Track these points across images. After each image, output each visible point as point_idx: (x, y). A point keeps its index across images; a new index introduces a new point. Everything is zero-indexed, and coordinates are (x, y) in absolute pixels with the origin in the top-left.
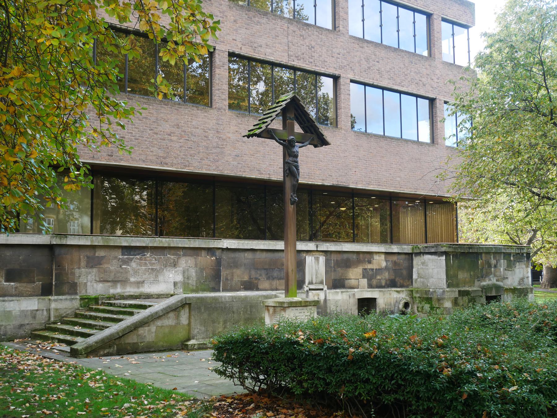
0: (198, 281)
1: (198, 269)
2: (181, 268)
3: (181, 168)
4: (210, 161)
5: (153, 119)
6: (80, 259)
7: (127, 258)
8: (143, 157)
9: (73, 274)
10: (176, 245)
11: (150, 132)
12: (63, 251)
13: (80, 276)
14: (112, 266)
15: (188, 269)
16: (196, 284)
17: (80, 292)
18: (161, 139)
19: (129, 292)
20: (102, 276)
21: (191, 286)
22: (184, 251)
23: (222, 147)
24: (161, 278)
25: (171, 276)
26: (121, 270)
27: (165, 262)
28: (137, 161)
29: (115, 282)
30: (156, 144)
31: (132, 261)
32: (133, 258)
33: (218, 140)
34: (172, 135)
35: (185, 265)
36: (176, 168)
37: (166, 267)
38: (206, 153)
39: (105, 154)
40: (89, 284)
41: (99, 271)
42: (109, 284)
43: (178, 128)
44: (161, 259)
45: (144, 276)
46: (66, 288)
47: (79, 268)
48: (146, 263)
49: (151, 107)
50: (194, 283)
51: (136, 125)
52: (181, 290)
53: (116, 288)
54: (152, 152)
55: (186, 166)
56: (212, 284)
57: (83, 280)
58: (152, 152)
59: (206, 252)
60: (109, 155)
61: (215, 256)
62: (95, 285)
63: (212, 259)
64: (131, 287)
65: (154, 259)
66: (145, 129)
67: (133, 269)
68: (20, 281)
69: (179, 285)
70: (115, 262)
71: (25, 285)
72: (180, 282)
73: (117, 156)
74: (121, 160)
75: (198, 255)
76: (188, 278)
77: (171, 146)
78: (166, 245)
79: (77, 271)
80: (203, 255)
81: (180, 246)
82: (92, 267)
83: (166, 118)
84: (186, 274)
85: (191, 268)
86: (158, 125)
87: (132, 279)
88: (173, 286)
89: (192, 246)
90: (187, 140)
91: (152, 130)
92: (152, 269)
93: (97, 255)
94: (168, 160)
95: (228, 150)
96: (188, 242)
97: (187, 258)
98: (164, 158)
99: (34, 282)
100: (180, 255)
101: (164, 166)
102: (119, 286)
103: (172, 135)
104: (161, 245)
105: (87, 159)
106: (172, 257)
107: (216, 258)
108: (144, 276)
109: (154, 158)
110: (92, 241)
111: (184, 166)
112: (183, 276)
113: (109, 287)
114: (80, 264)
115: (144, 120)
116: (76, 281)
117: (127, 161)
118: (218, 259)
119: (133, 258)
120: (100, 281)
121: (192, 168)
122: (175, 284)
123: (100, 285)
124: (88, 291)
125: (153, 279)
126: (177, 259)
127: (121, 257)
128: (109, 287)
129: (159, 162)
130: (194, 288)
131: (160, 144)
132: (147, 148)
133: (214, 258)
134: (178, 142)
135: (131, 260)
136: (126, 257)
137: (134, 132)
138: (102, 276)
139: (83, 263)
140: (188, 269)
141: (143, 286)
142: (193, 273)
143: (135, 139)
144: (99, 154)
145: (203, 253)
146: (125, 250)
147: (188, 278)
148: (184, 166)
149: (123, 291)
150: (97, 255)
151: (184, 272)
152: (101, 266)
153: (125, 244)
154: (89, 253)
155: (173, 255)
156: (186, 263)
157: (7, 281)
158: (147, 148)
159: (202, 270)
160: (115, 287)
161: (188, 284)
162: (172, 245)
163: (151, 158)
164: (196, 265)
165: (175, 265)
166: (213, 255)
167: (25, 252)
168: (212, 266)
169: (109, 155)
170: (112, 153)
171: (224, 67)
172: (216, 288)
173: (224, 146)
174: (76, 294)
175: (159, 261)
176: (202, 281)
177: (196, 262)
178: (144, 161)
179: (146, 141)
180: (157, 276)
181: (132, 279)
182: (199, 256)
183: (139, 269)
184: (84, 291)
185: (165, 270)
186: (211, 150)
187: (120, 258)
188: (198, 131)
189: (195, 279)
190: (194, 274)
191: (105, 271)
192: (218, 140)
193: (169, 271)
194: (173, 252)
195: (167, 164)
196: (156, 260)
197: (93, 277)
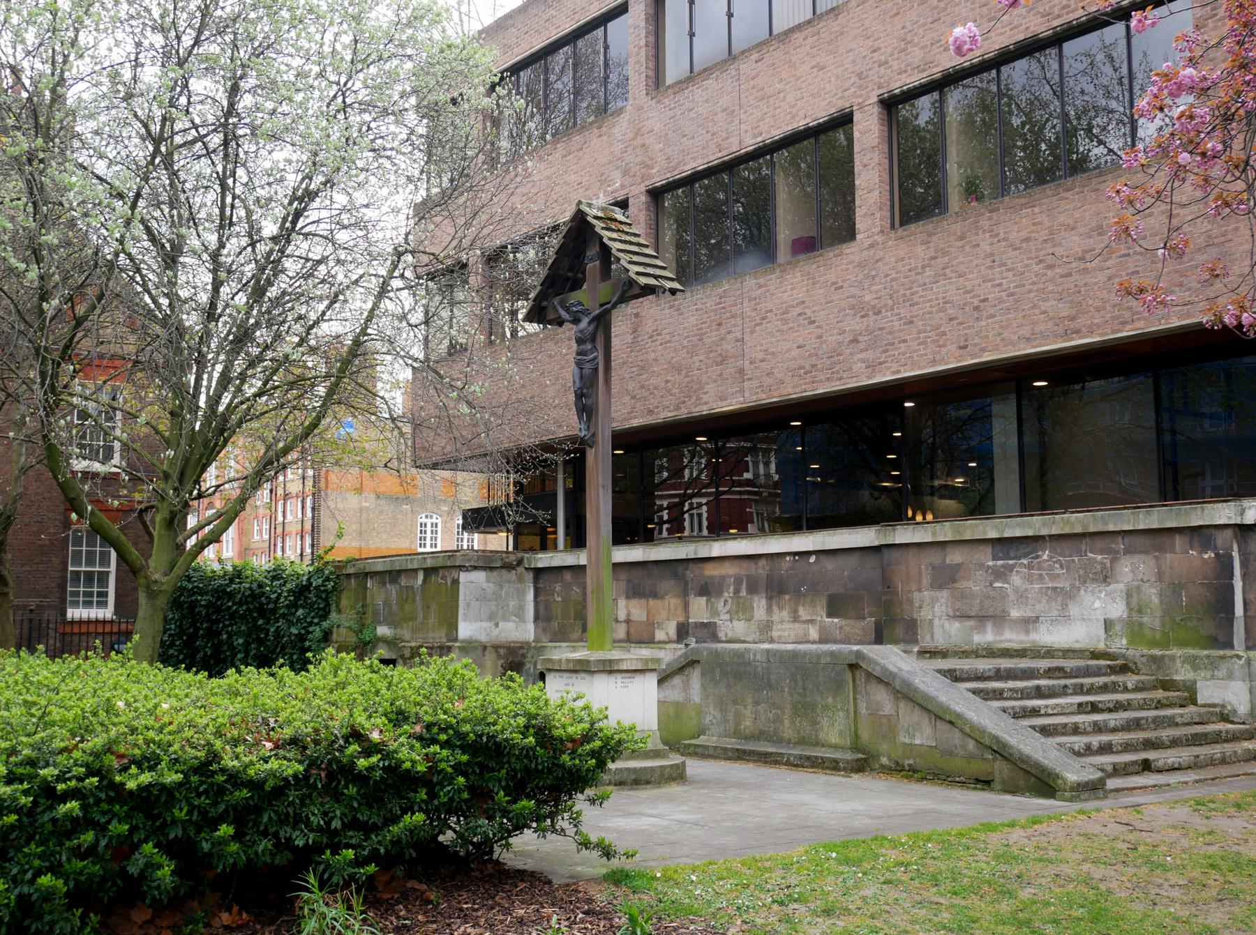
0: (1167, 619)
1: (1164, 586)
2: (1121, 586)
3: (1113, 332)
4: (1189, 289)
5: (1043, 235)
6: (920, 573)
7: (1003, 566)
8: (1025, 332)
9: (910, 601)
10: (1100, 528)
11: (1036, 268)
12: (895, 554)
13: (921, 607)
14: (975, 585)
15: (1138, 588)
16: (1163, 625)
17: (923, 638)
18: (1062, 276)
19: (1010, 641)
20: (959, 605)
21: (1147, 632)
22: (1127, 540)
23: (1222, 239)
24: (1074, 610)
25: (1097, 604)
26: (992, 593)
27: (1082, 572)
28: (1013, 344)
29: (982, 619)
30: (1052, 292)
31: (1011, 571)
32: (1013, 566)
33: (1209, 227)
34: (1088, 257)
35: (1131, 575)
36: (1101, 335)
37: (1085, 582)
38: (1176, 272)
39: (953, 348)
40: (936, 622)
41: (953, 596)
42: (972, 623)
43: (1100, 234)
44: (1072, 565)
45: (1037, 607)
46: (899, 631)
47: (920, 590)
48: (1041, 575)
49: (1037, 210)
50: (1157, 624)
51: (1009, 262)
52: (1124, 642)
53: (984, 632)
54: (1044, 312)
55: (1125, 323)
56: (1208, 627)
57: (925, 614)
58: (1044, 312)
59: (1187, 539)
60: (961, 348)
61: (1215, 549)
62: (947, 624)
63: (1206, 556)
64: (1012, 629)
65: (1057, 566)
66: (1026, 266)
67: (1016, 591)
68: (846, 618)
69: (1118, 627)
70: (980, 574)
71: (851, 622)
72: (1120, 620)
73: (975, 345)
74: (983, 350)
75: (1162, 549)
76: (1140, 611)
77: (1085, 285)
78: (1078, 529)
79: (916, 595)
80: (1178, 549)
81: (1111, 528)
82: (940, 587)
83: (1071, 221)
84: (1135, 600)
85: (1147, 585)
86: (1054, 246)
87: (1015, 613)
88: (1103, 631)
89: (1141, 527)
90: (1124, 255)
91: (1041, 261)
92: (1054, 589)
93: (948, 561)
94: (1083, 321)
95: (1241, 244)
96: (1132, 517)
97: (1137, 558)
98: (1073, 319)
99: (864, 618)
100: (1117, 552)
101: (1073, 339)
102: (989, 626)
103: (1088, 257)
104: (1067, 530)
105: (923, 368)
106: (1099, 557)
107: (1217, 555)
108: (1037, 607)
109: (1050, 324)
110: (934, 534)
111: (1121, 323)
112: (1128, 604)
113: (972, 628)
114: (920, 582)
115: (1024, 245)
116: (915, 616)
117: (996, 348)
118: (1222, 556)
119: (1013, 566)
120: (955, 617)
121: (1141, 324)
122: (1108, 625)
123: (957, 624)
124: (936, 637)
125: (1056, 613)
126: (1112, 561)
127: (991, 563)
128: (972, 628)
129: (1061, 331)
130: (1158, 636)
131: (1060, 288)
132: (1033, 308)
133: (1209, 555)
134: (1101, 269)
135: (1011, 568)
136: (1000, 562)
137: (1004, 281)
138: (959, 605)
139: (926, 580)
140: (1138, 588)
141: (1036, 629)
142: (1152, 594)
143: (1008, 296)
144: (944, 350)
145: (1179, 541)
146: (998, 548)
147: (1140, 611)
148: (1121, 323)
149: (998, 638)
150: (948, 561)
151: (1129, 595)
152: (956, 585)
153: (993, 534)
154: (934, 557)
155: (1101, 552)
156: (1132, 571)
157: (830, 615)
158: (1033, 308)
159: (1176, 588)
160: (981, 628)
161: (1141, 625)
162: (1092, 529)
163: (1042, 327)
164: (1160, 576)
165: (1105, 577)
166: (1206, 545)
167: (852, 561)
168: (1205, 578)
169: (961, 348)
170: (966, 340)
171: (1215, 15)
172: (1221, 639)
173: (1229, 237)
174: (916, 642)
175: (1068, 569)
176: (1178, 619)
177: (1159, 567)
178: (1028, 339)
179: (1030, 291)
180: (1064, 606)
181: (1015, 613)
182: (1166, 552)
183: (1026, 590)
184: (928, 637)
185: (1082, 592)
186: (1192, 260)
187: (989, 567)
188: (1152, 221)
189: (1158, 613)
190: (1155, 600)
191: (963, 596)
192: (1209, 227)
193: (1093, 592)
194: (1100, 543)
195: (1078, 331)
196: (1062, 567)
197: (943, 608)
